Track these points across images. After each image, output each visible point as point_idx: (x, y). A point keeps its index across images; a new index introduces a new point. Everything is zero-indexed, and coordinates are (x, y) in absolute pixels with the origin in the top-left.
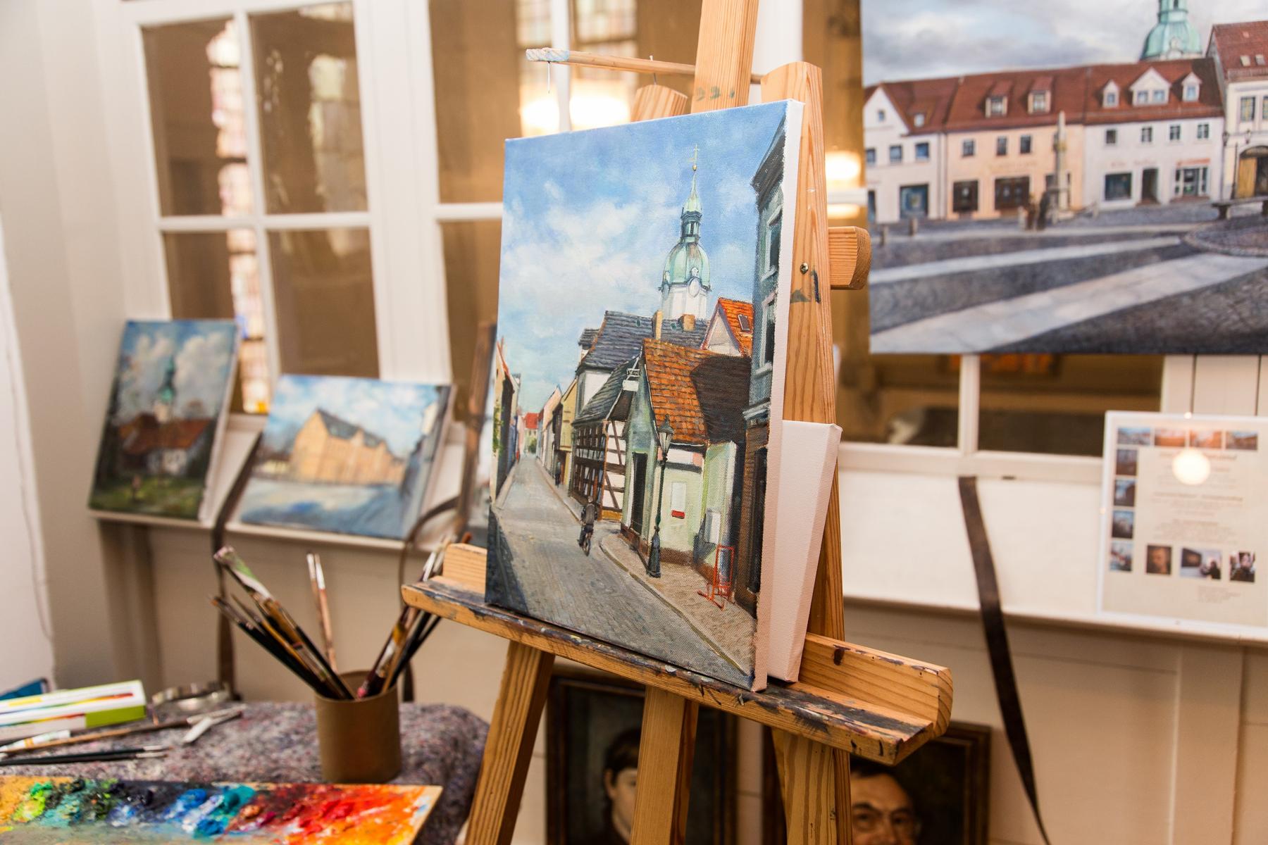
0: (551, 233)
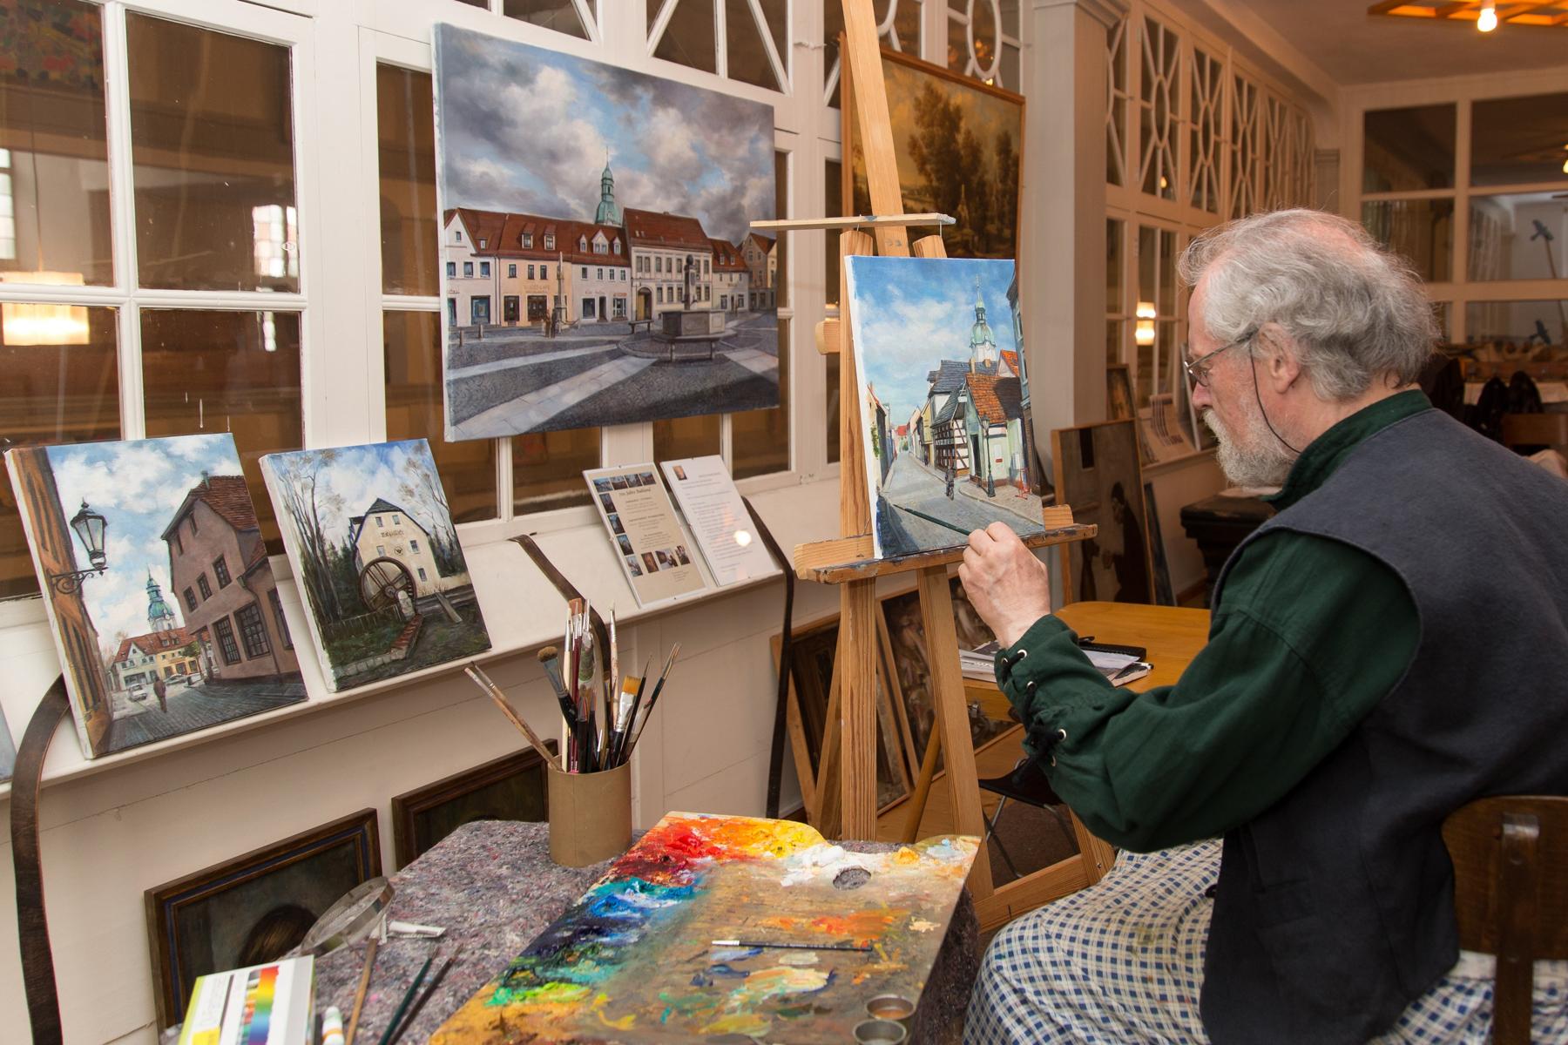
0: (897, 315)
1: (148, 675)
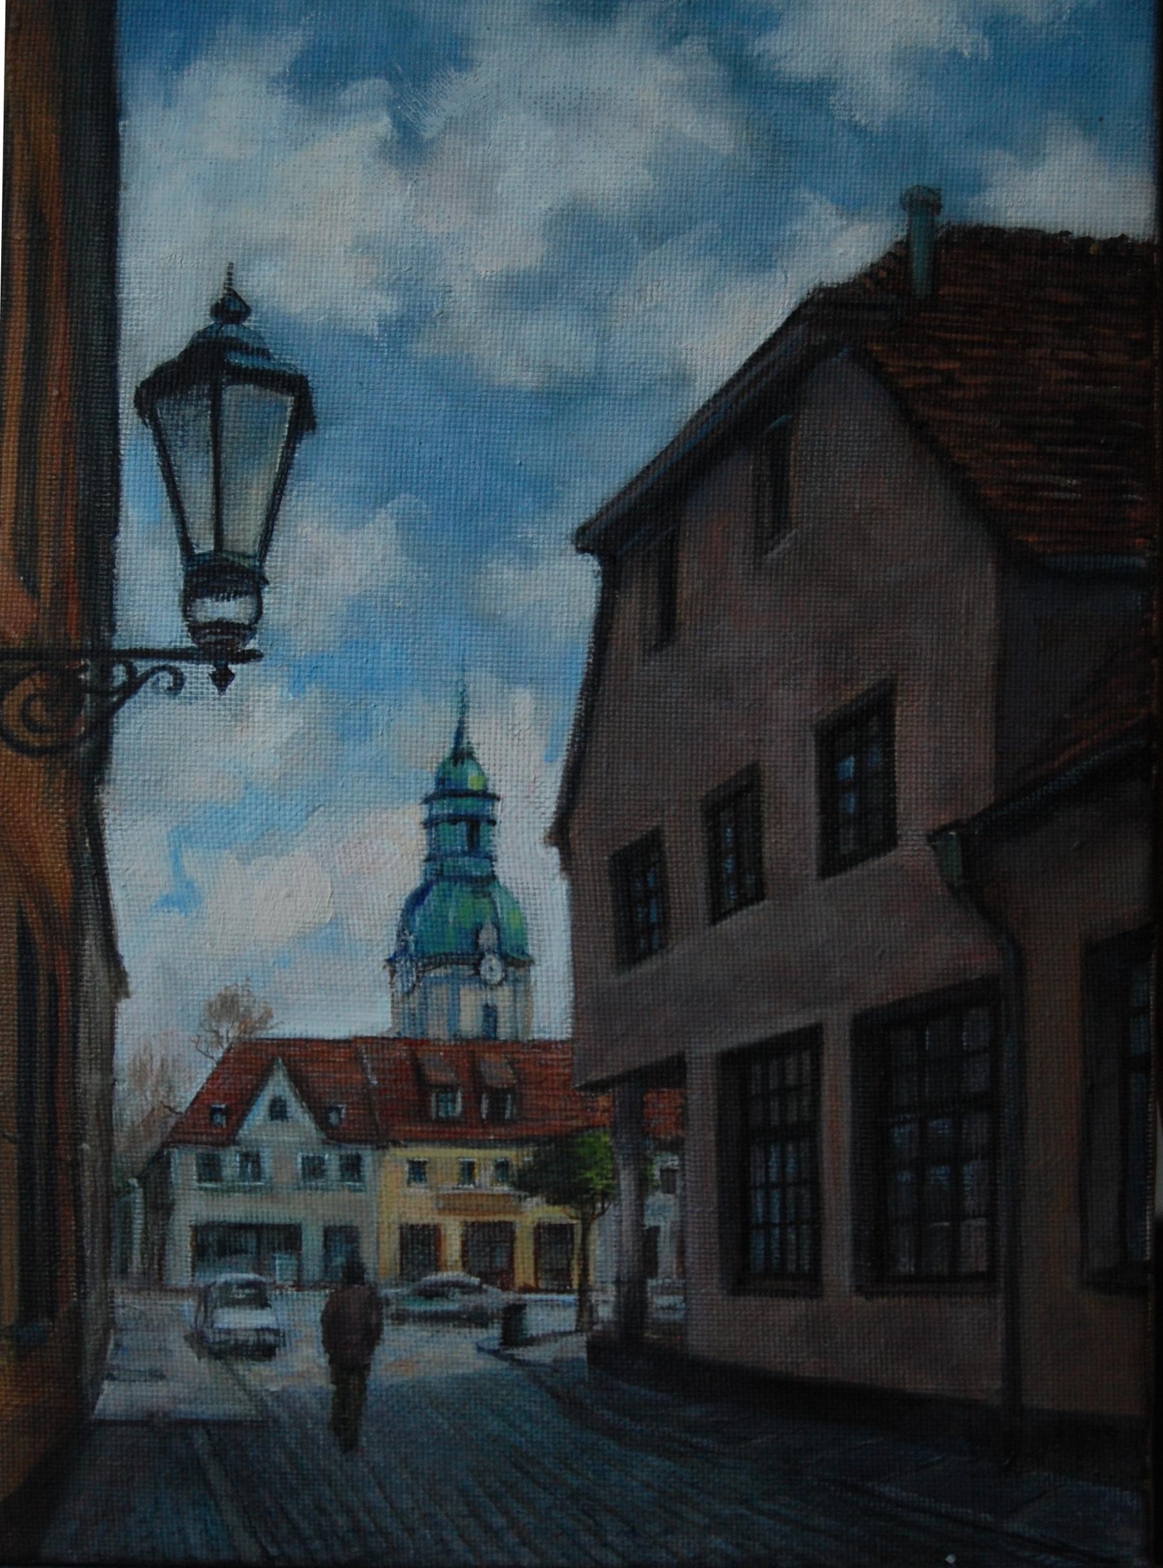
1: (312, 1241)
